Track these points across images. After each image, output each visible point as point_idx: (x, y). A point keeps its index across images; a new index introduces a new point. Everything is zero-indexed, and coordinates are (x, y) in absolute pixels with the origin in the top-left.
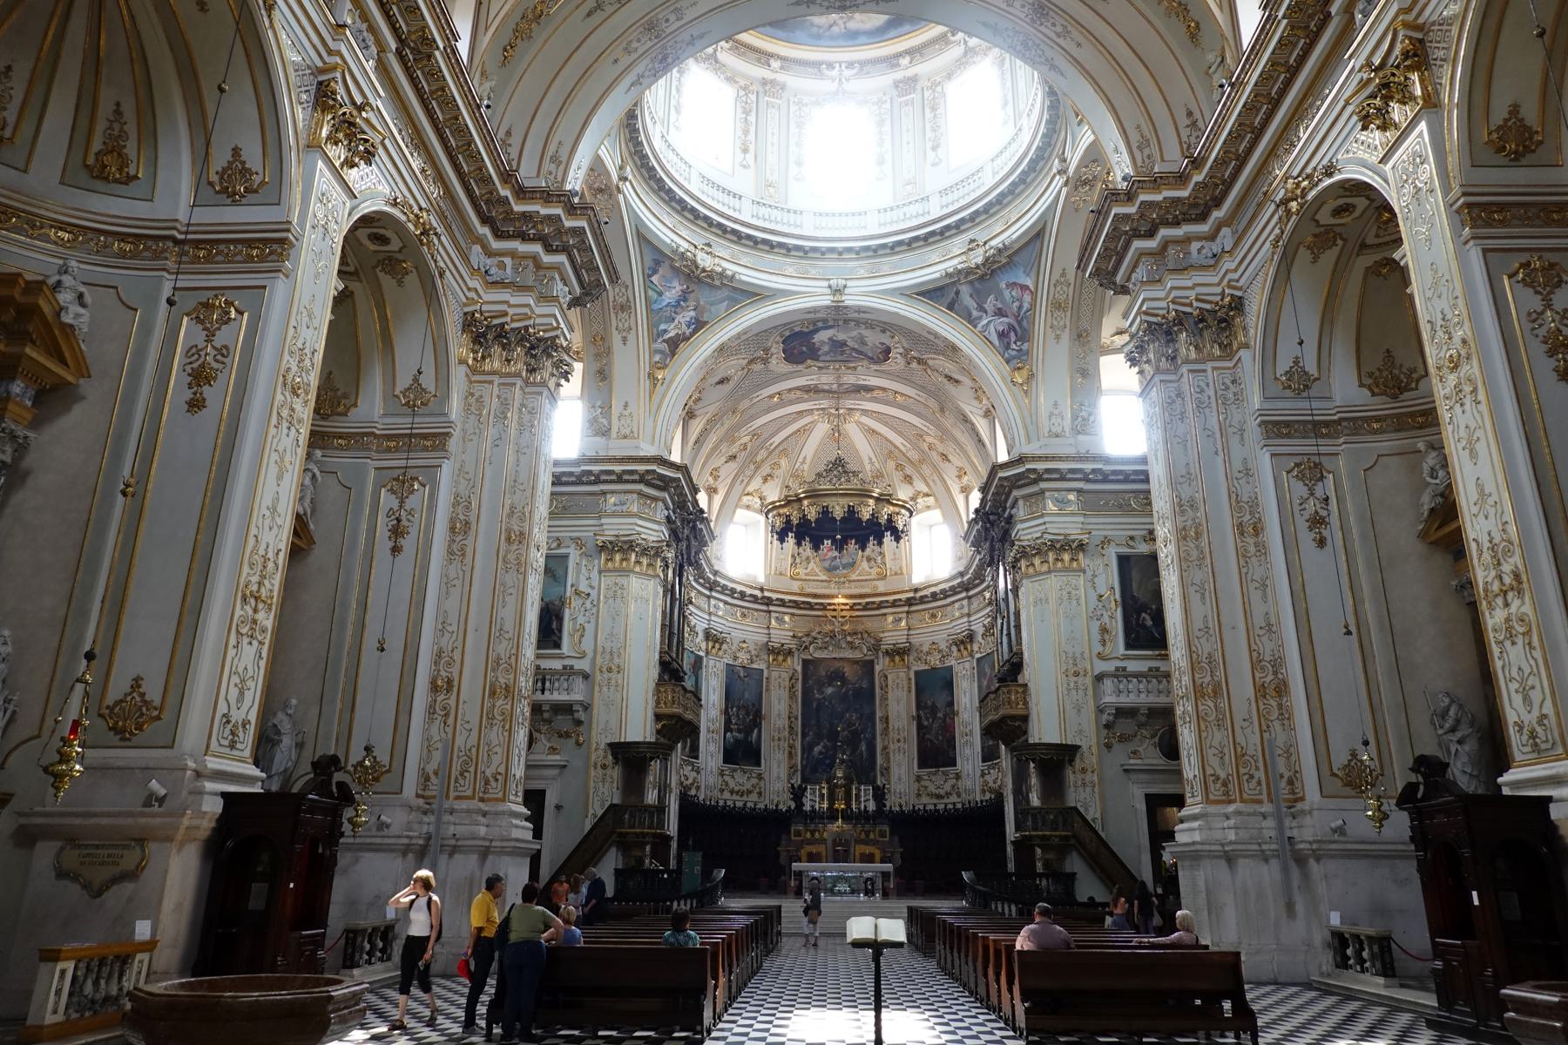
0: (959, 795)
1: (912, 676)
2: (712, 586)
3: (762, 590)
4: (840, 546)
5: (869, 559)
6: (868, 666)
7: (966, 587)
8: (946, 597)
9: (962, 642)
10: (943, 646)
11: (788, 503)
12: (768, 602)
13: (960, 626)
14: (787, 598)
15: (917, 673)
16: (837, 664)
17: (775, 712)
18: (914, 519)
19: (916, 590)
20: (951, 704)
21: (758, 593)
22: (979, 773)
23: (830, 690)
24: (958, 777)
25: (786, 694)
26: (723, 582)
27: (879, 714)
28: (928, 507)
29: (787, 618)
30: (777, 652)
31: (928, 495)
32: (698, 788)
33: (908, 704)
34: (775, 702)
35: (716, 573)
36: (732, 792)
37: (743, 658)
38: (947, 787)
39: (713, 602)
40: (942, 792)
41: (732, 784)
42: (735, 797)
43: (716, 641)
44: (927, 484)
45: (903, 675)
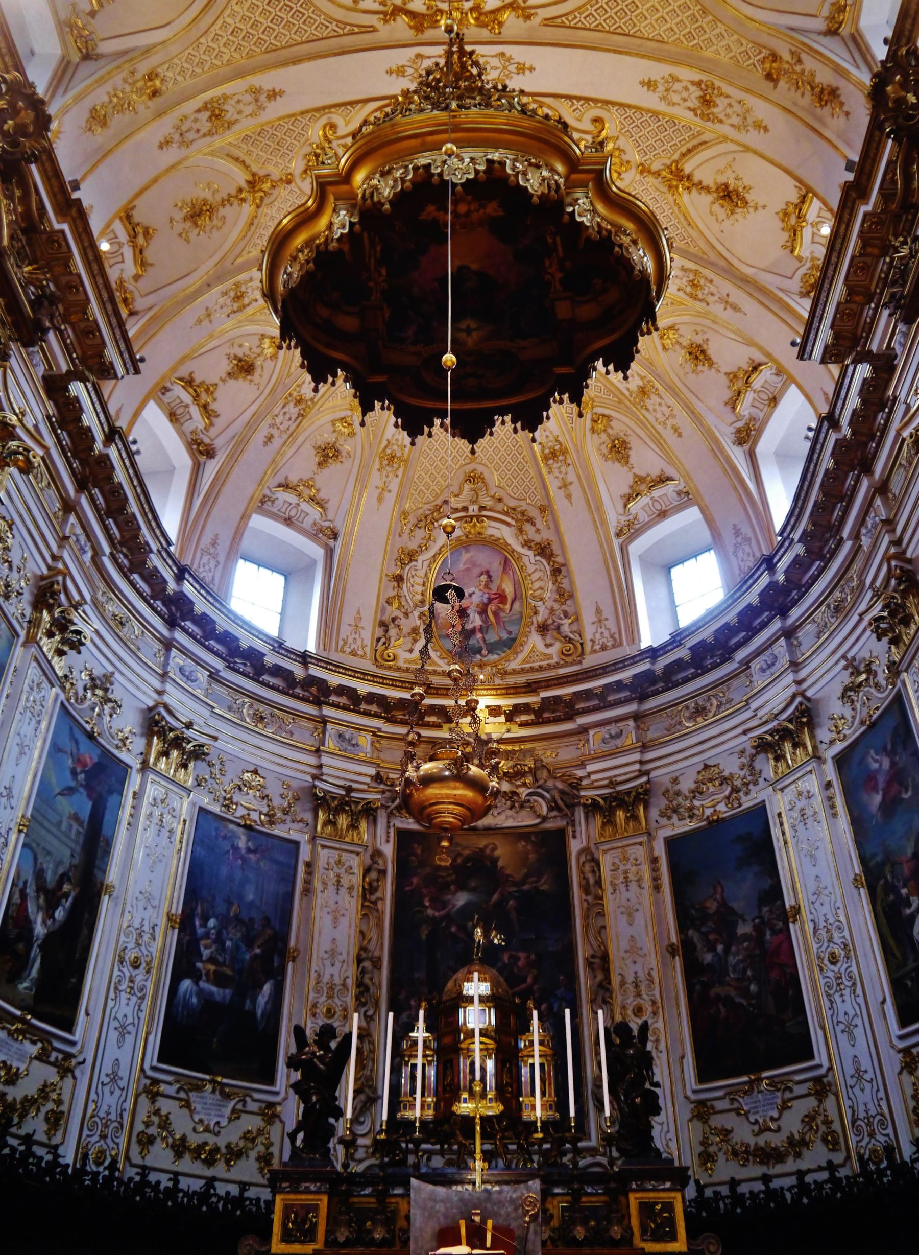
0: (832, 1142)
1: (660, 850)
2: (177, 610)
3: (304, 658)
4: (471, 428)
5: (543, 629)
6: (550, 846)
7: (778, 601)
8: (727, 658)
9: (783, 734)
10: (731, 766)
11: (322, 188)
12: (318, 693)
13: (776, 697)
14: (364, 688)
15: (671, 843)
16: (482, 842)
17: (321, 944)
18: (636, 548)
19: (653, 653)
20: (773, 893)
21: (298, 671)
22: (892, 1062)
23: (461, 899)
24: (822, 1087)
25: (351, 905)
26: (201, 606)
27: (582, 952)
28: (663, 515)
29: (365, 740)
30: (335, 807)
31: (663, 480)
32: (56, 1120)
33: (658, 917)
34: (322, 920)
35: (182, 573)
36: (180, 1148)
37: (248, 805)
38: (792, 1123)
39: (177, 659)
40: (777, 1140)
41: (181, 1124)
42: (186, 1165)
43: (178, 742)
44: (659, 442)
45: (639, 853)
